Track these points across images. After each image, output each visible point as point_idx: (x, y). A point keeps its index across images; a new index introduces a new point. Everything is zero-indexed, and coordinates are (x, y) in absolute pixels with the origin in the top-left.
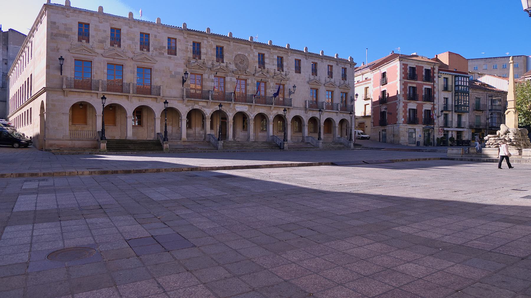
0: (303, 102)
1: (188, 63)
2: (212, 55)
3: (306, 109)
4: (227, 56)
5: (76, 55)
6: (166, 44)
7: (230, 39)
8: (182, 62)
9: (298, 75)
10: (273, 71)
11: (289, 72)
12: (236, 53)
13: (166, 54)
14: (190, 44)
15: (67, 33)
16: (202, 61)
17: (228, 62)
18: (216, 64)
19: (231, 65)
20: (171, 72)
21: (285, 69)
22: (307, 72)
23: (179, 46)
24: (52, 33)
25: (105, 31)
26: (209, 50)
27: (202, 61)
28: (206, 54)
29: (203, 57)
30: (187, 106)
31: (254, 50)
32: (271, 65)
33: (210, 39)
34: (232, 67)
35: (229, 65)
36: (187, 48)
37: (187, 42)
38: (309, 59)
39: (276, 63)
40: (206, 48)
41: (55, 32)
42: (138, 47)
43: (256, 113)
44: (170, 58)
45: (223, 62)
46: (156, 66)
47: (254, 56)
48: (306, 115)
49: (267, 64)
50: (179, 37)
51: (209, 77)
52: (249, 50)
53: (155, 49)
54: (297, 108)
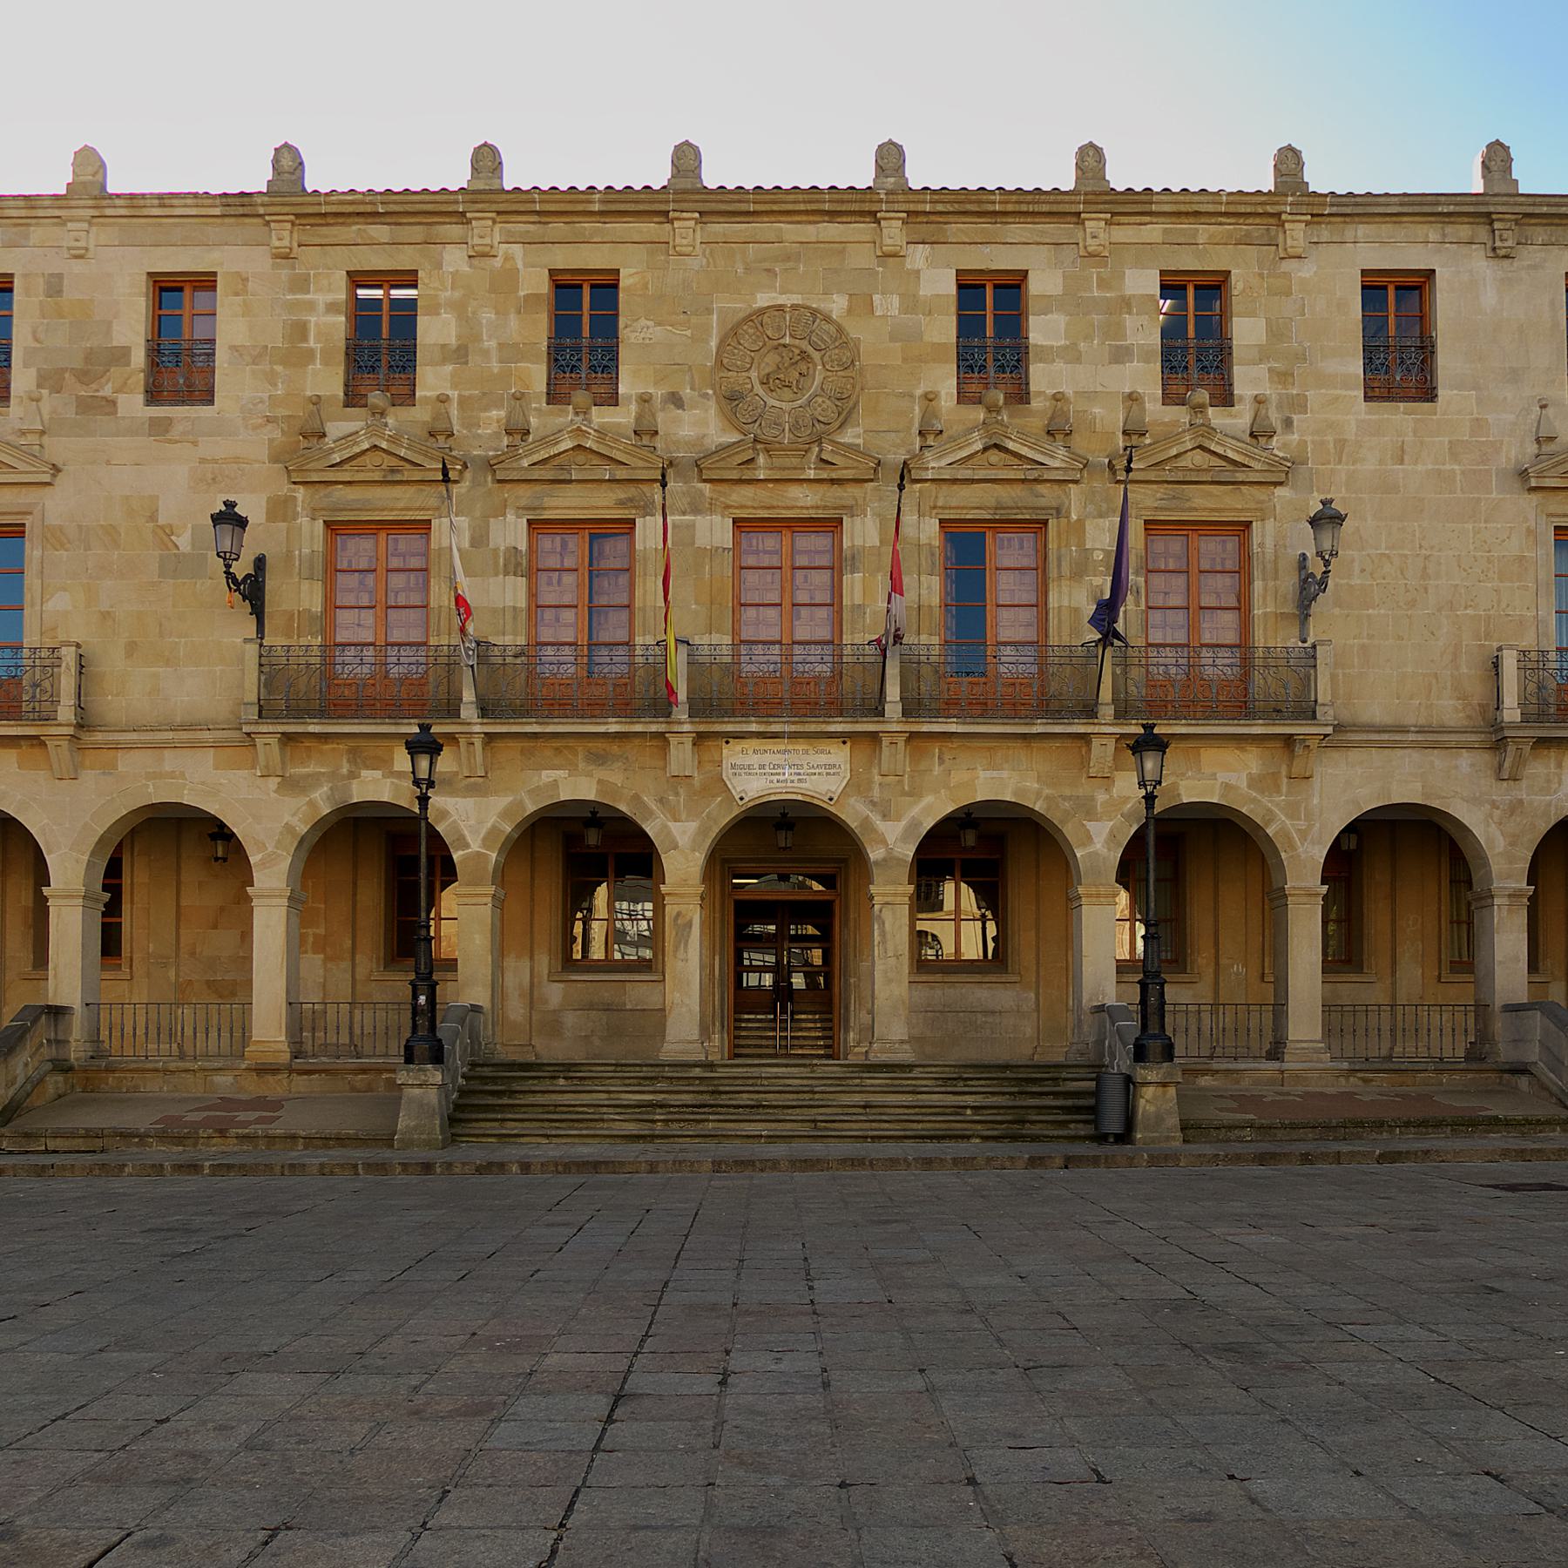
2: (512, 352)
3: (1495, 738)
6: (131, 329)
7: (685, 198)
9: (1400, 417)
10: (1110, 418)
11: (1300, 404)
12: (732, 305)
13: (133, 404)
14: (321, 299)
16: (419, 414)
17: (658, 393)
18: (541, 418)
19: (684, 415)
21: (1247, 379)
22: (1515, 376)
23: (232, 327)
26: (487, 316)
27: (419, 414)
28: (459, 354)
29: (431, 379)
30: (291, 785)
31: (918, 256)
32: (1094, 357)
33: (486, 232)
34: (699, 426)
36: (301, 330)
37: (301, 284)
38: (1530, 255)
39: (1145, 333)
40: (459, 308)
43: (932, 808)
44: (159, 428)
45: (613, 400)
46: (54, 507)
47: (911, 303)
48: (1502, 793)
49: (1048, 354)
52: (862, 257)
53: (51, 380)
54: (1390, 736)
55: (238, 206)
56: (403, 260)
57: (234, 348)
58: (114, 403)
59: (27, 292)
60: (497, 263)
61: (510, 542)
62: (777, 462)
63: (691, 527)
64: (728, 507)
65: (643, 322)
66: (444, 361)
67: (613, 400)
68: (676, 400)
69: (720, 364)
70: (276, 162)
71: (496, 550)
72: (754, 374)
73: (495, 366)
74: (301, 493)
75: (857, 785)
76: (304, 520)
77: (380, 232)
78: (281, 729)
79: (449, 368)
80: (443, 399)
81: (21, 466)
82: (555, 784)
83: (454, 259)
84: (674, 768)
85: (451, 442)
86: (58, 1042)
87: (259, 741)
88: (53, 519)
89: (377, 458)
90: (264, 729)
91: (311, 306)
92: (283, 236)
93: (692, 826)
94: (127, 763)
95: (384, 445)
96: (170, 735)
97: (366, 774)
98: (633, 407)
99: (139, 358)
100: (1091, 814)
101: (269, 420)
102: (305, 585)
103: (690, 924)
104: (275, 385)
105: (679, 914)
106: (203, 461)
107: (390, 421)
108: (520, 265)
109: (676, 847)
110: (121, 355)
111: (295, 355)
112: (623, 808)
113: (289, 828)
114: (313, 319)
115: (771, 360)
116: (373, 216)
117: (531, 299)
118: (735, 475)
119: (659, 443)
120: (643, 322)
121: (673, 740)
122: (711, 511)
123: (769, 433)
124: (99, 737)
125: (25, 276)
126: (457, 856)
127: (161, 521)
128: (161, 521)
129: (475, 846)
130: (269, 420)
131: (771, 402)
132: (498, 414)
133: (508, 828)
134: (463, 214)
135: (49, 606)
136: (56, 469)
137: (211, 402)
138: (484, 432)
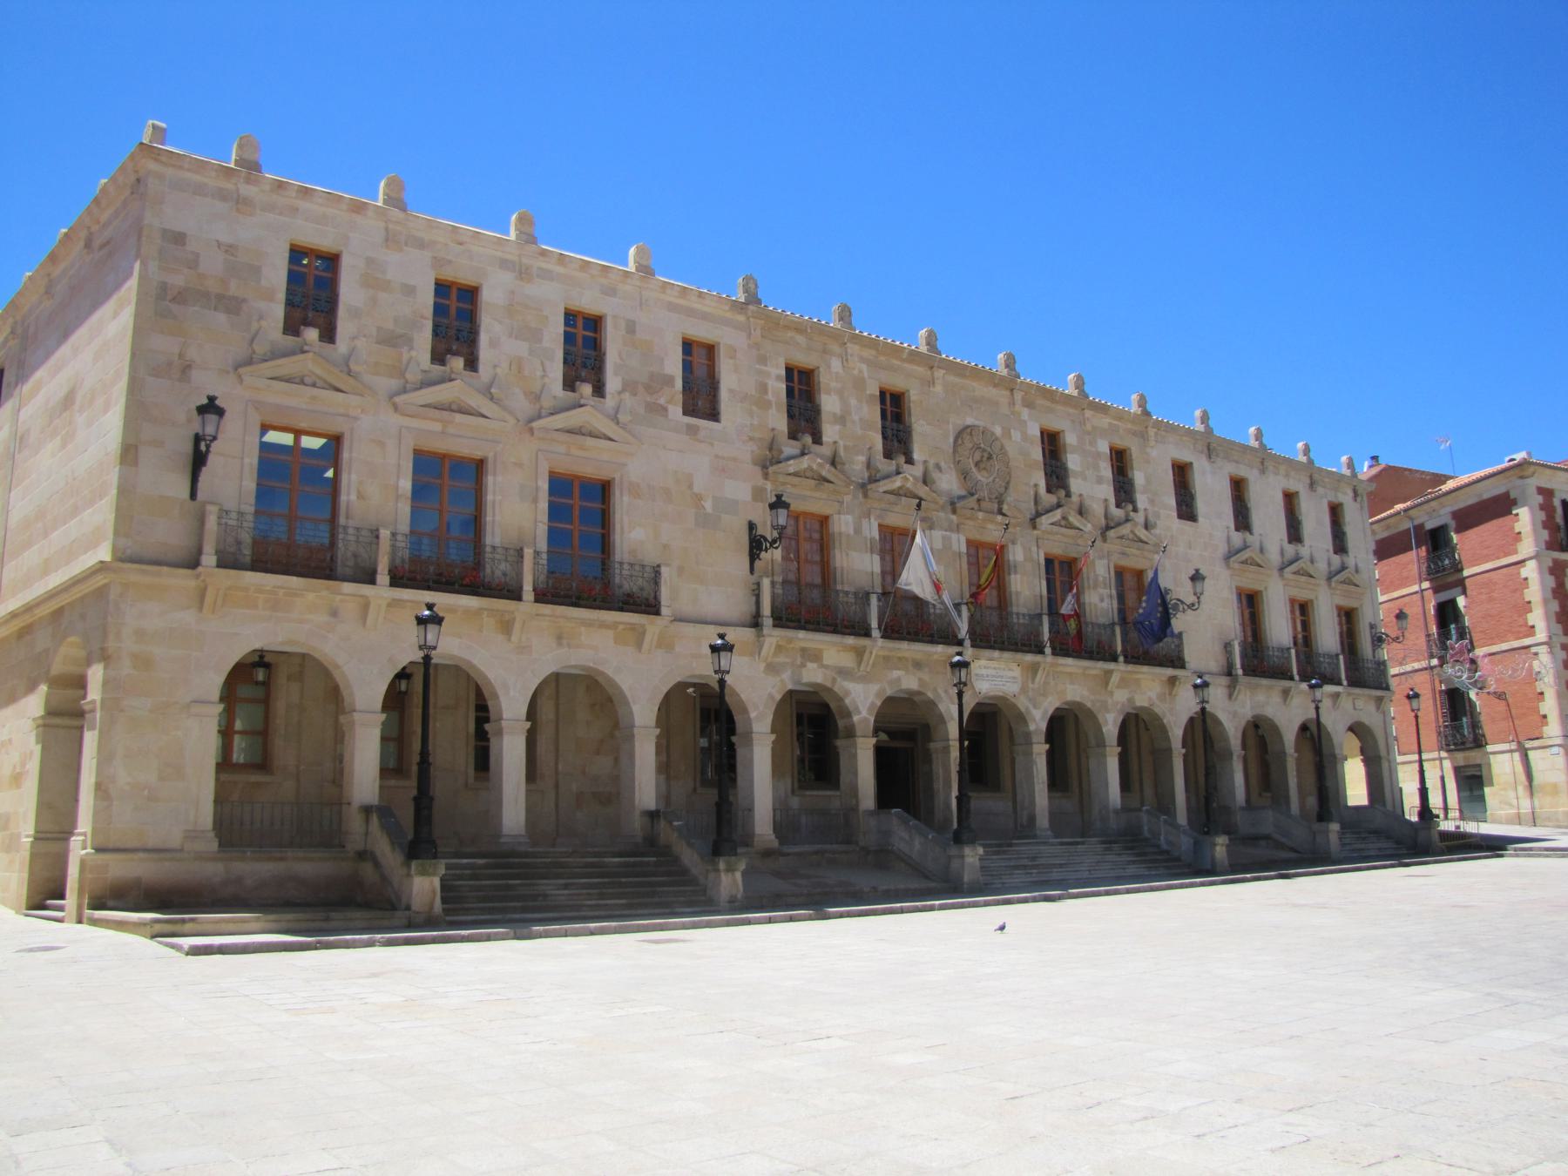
0: (1218, 648)
1: (769, 460)
4: (928, 437)
6: (673, 366)
8: (745, 452)
11: (1157, 515)
13: (676, 411)
15: (234, 289)
16: (825, 450)
18: (884, 466)
20: (698, 498)
21: (1142, 500)
23: (729, 379)
24: (164, 287)
25: (409, 290)
26: (853, 402)
27: (825, 450)
28: (842, 420)
29: (830, 432)
30: (771, 668)
31: (1025, 413)
32: (1091, 483)
34: (948, 482)
35: (935, 475)
36: (763, 388)
37: (763, 360)
40: (840, 393)
41: (178, 280)
42: (556, 370)
44: (692, 431)
47: (1025, 437)
51: (858, 531)
53: (629, 387)
57: (731, 391)
58: (666, 409)
75: (1024, 690)
79: (837, 427)
82: (899, 679)
97: (811, 665)
99: (679, 384)
100: (1108, 711)
101: (751, 439)
110: (669, 381)
112: (930, 695)
113: (771, 696)
115: (977, 456)
117: (872, 396)
125: (614, 317)
127: (696, 490)
128: (696, 490)
130: (751, 439)
133: (879, 703)
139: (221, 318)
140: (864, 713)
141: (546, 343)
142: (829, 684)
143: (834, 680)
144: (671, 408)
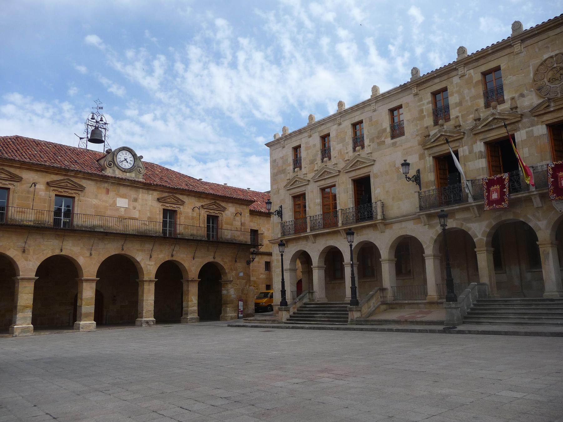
5: (293, 191)
13: (389, 141)
14: (425, 102)
16: (452, 123)
17: (516, 95)
19: (526, 99)
26: (466, 91)
27: (452, 123)
28: (460, 104)
29: (454, 113)
30: (431, 226)
36: (422, 111)
37: (421, 100)
44: (394, 144)
45: (503, 102)
50: (406, 99)
51: (471, 152)
53: (372, 140)
55: (404, 88)
56: (442, 85)
57: (408, 121)
58: (384, 141)
59: (366, 122)
60: (467, 76)
61: (479, 150)
62: (558, 103)
63: (532, 131)
64: (542, 122)
65: (509, 77)
66: (456, 107)
67: (503, 102)
68: (522, 95)
69: (534, 81)
70: (412, 73)
71: (476, 153)
72: (545, 80)
73: (469, 104)
74: (426, 152)
76: (427, 158)
77: (437, 80)
78: (425, 213)
80: (457, 117)
81: (368, 162)
83: (456, 80)
84: (535, 205)
85: (461, 128)
86: (383, 297)
87: (421, 217)
88: (375, 172)
89: (443, 137)
90: (421, 213)
91: (423, 104)
92: (415, 90)
93: (545, 222)
94: (396, 227)
95: (443, 134)
96: (402, 218)
98: (509, 102)
99: (388, 129)
101: (417, 135)
102: (429, 174)
103: (548, 253)
104: (417, 126)
105: (544, 251)
106: (404, 149)
107: (445, 127)
108: (473, 74)
109: (540, 229)
110: (385, 130)
111: (421, 117)
112: (522, 219)
113: (432, 238)
114: (424, 107)
115: (550, 74)
116: (434, 78)
117: (477, 82)
118: (543, 112)
119: (518, 110)
120: (509, 77)
121: (533, 198)
122: (537, 124)
123: (552, 96)
124: (388, 221)
126: (475, 240)
129: (480, 236)
130: (417, 135)
131: (552, 86)
132: (472, 116)
133: (488, 230)
134: (455, 68)
135: (376, 192)
136: (374, 161)
137: (404, 135)
138: (468, 123)
139: (283, 175)
140: (480, 236)
141: (347, 140)
142: (459, 227)
143: (462, 225)
144: (386, 140)
